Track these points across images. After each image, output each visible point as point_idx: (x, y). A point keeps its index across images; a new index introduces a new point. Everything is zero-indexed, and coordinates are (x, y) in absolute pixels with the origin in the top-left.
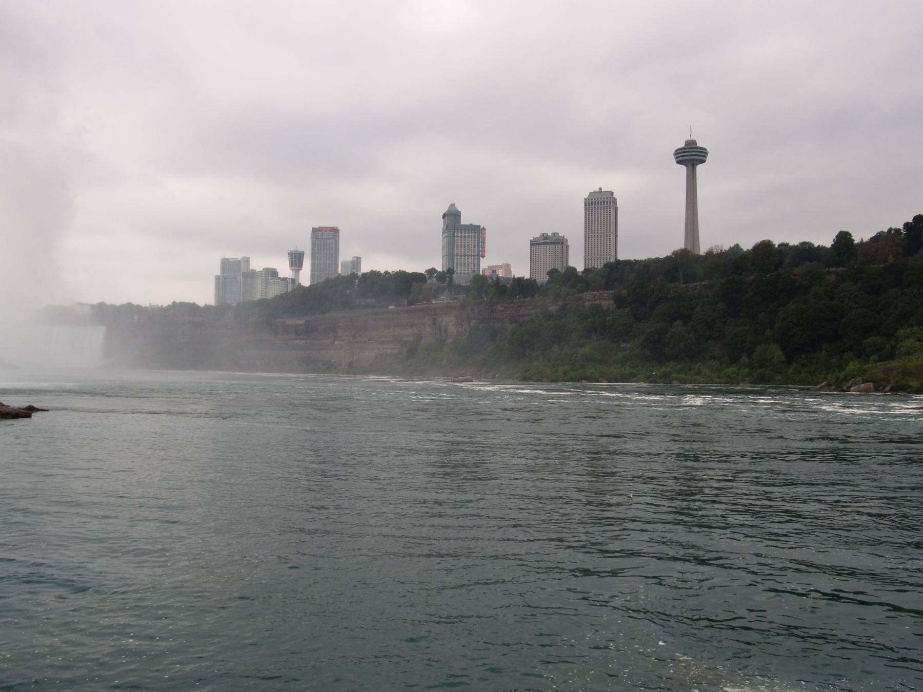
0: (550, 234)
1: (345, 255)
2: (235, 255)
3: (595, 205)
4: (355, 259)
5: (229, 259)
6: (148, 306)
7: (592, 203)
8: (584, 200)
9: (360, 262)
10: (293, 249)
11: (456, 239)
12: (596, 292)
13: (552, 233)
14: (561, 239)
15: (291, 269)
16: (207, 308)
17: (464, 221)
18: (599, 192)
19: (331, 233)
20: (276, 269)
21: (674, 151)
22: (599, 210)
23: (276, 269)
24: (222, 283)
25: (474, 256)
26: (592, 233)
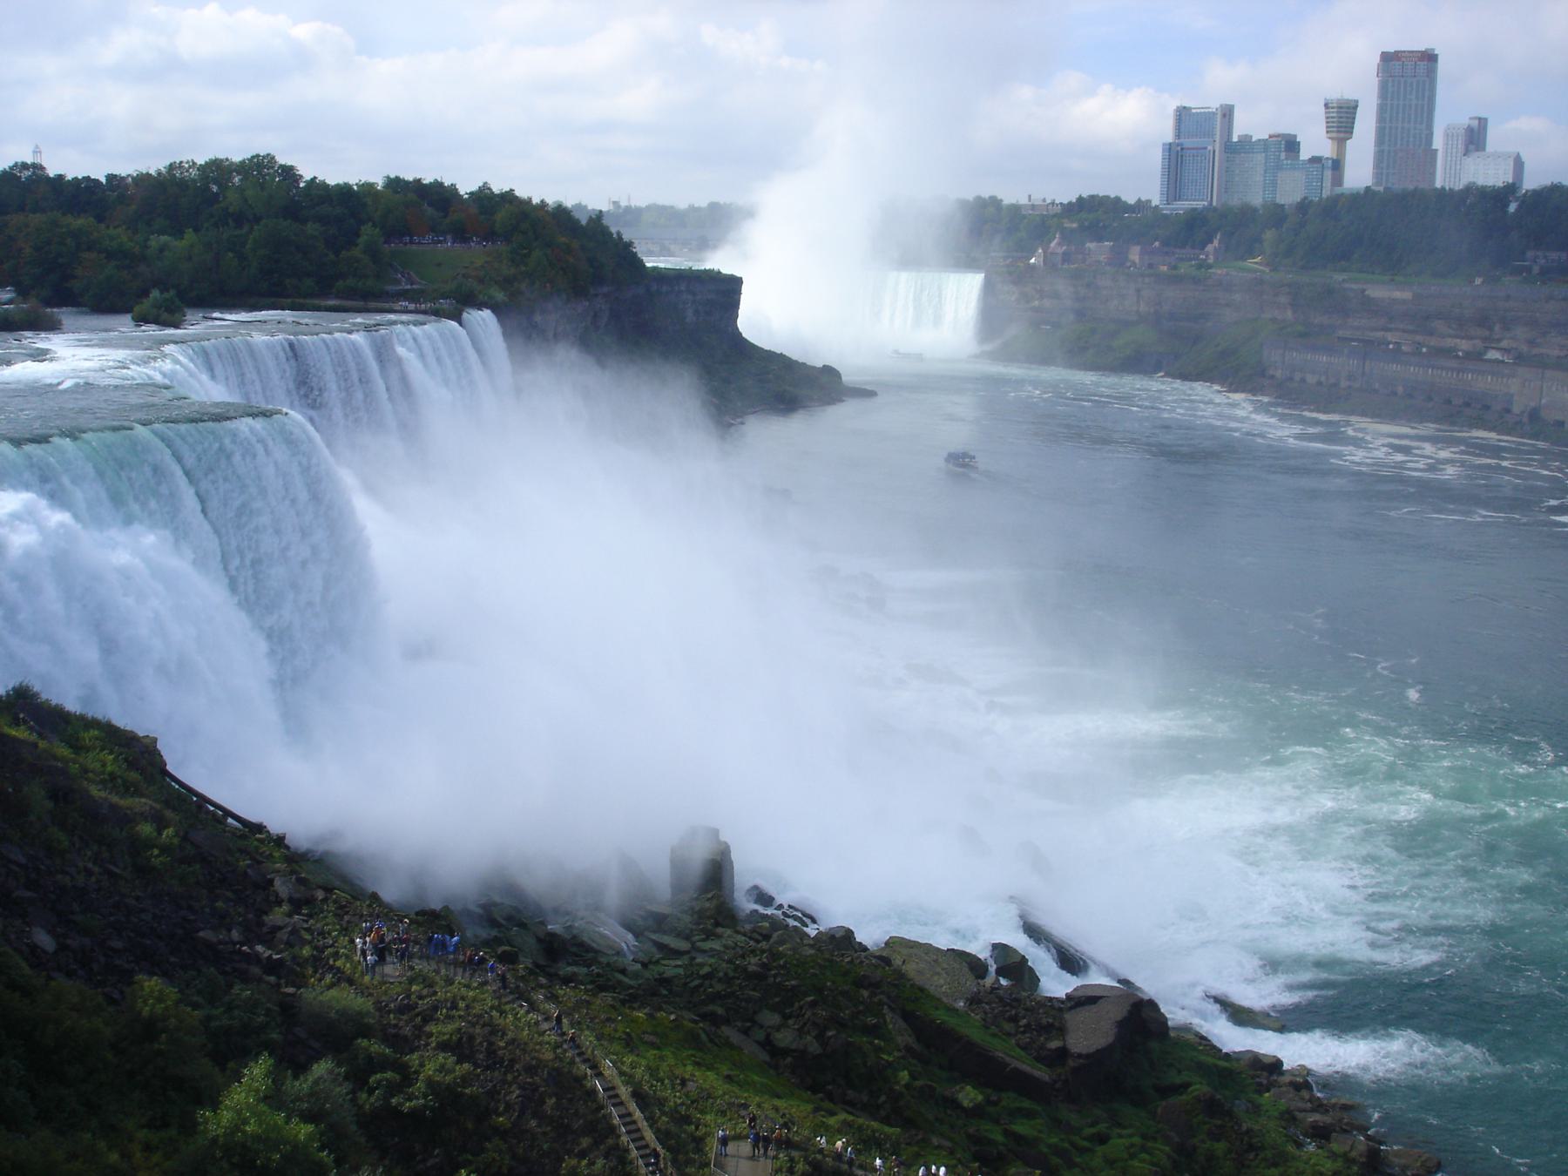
1: (1449, 114)
4: (1475, 123)
5: (1190, 109)
6: (1024, 201)
15: (1330, 138)
16: (1141, 206)
19: (1422, 63)
20: (1295, 136)
23: (1295, 136)
24: (1177, 159)
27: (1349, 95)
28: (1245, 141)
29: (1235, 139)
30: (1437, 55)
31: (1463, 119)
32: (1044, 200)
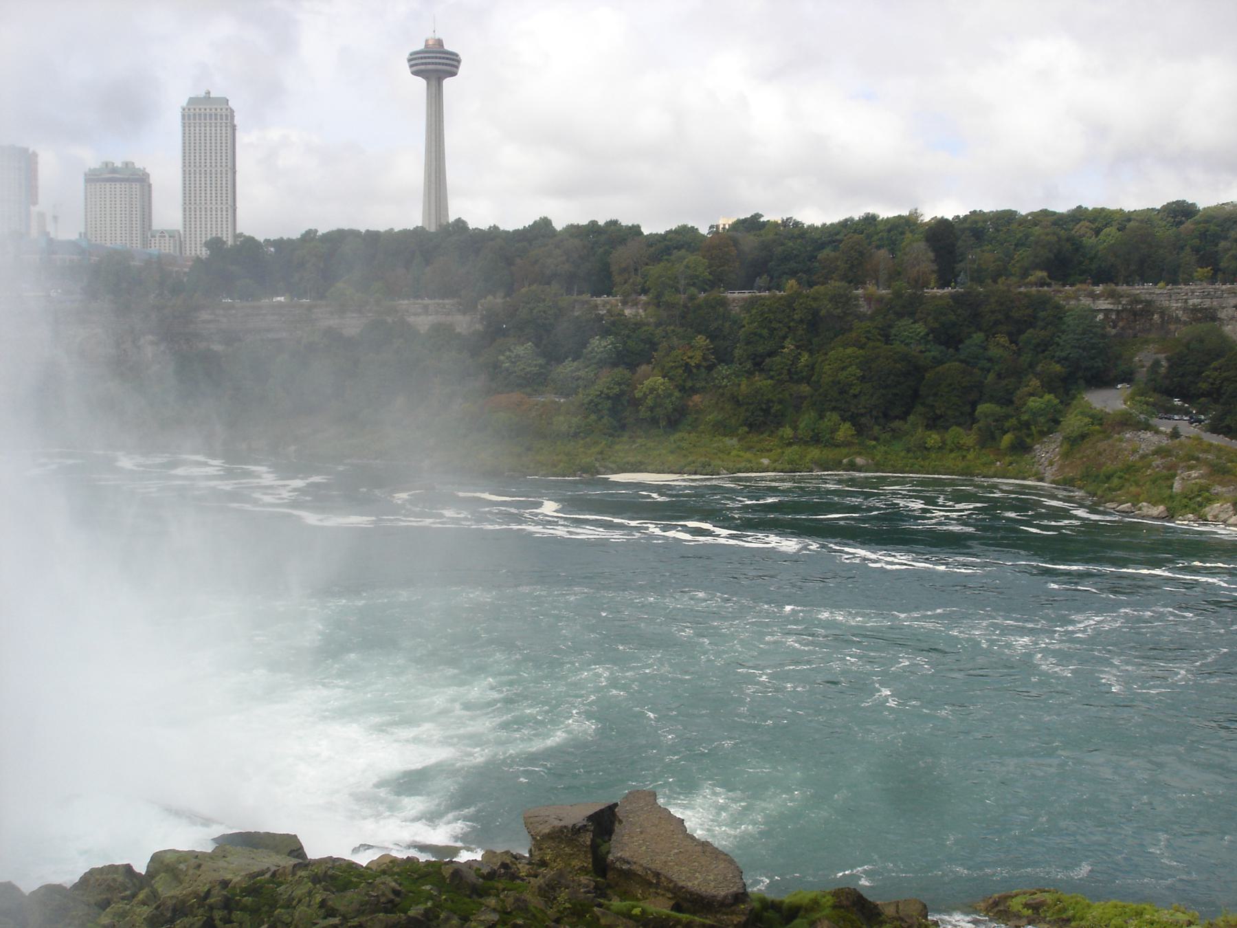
0: (118, 164)
3: (205, 119)
7: (194, 115)
8: (181, 110)
12: (427, 301)
13: (123, 163)
14: (141, 174)
18: (205, 97)
21: (407, 55)
22: (208, 128)
26: (195, 166)
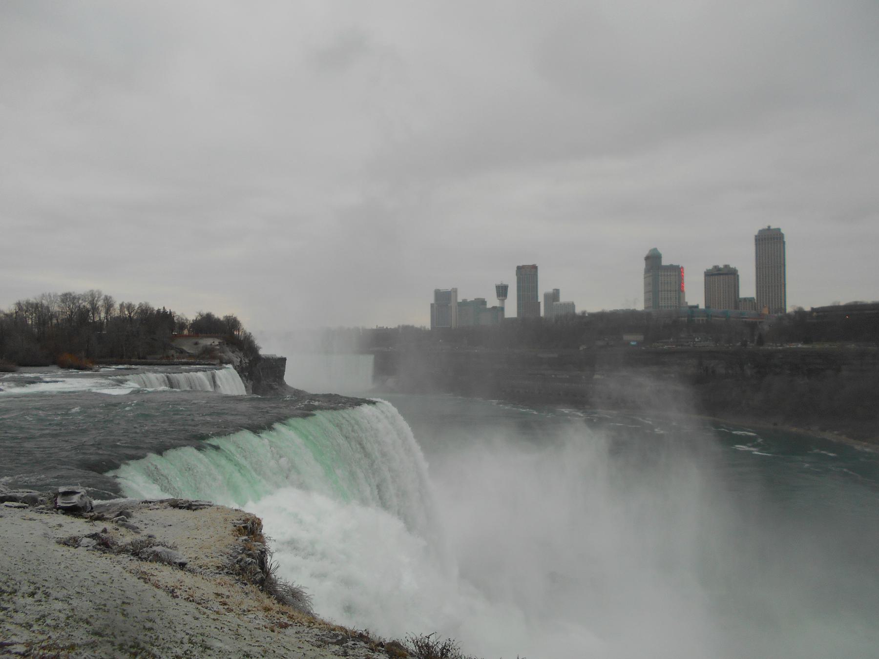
0: (721, 266)
1: (544, 288)
2: (445, 287)
5: (440, 290)
6: (375, 327)
8: (754, 237)
9: (559, 293)
10: (499, 283)
11: (660, 277)
15: (499, 299)
17: (665, 262)
20: (484, 299)
23: (484, 299)
25: (676, 291)
27: (505, 283)
28: (465, 303)
29: (460, 300)
30: (537, 267)
31: (550, 290)
32: (383, 327)
